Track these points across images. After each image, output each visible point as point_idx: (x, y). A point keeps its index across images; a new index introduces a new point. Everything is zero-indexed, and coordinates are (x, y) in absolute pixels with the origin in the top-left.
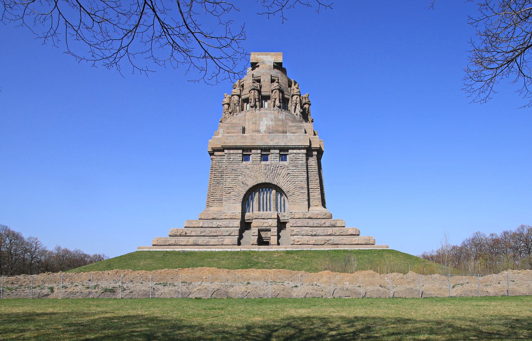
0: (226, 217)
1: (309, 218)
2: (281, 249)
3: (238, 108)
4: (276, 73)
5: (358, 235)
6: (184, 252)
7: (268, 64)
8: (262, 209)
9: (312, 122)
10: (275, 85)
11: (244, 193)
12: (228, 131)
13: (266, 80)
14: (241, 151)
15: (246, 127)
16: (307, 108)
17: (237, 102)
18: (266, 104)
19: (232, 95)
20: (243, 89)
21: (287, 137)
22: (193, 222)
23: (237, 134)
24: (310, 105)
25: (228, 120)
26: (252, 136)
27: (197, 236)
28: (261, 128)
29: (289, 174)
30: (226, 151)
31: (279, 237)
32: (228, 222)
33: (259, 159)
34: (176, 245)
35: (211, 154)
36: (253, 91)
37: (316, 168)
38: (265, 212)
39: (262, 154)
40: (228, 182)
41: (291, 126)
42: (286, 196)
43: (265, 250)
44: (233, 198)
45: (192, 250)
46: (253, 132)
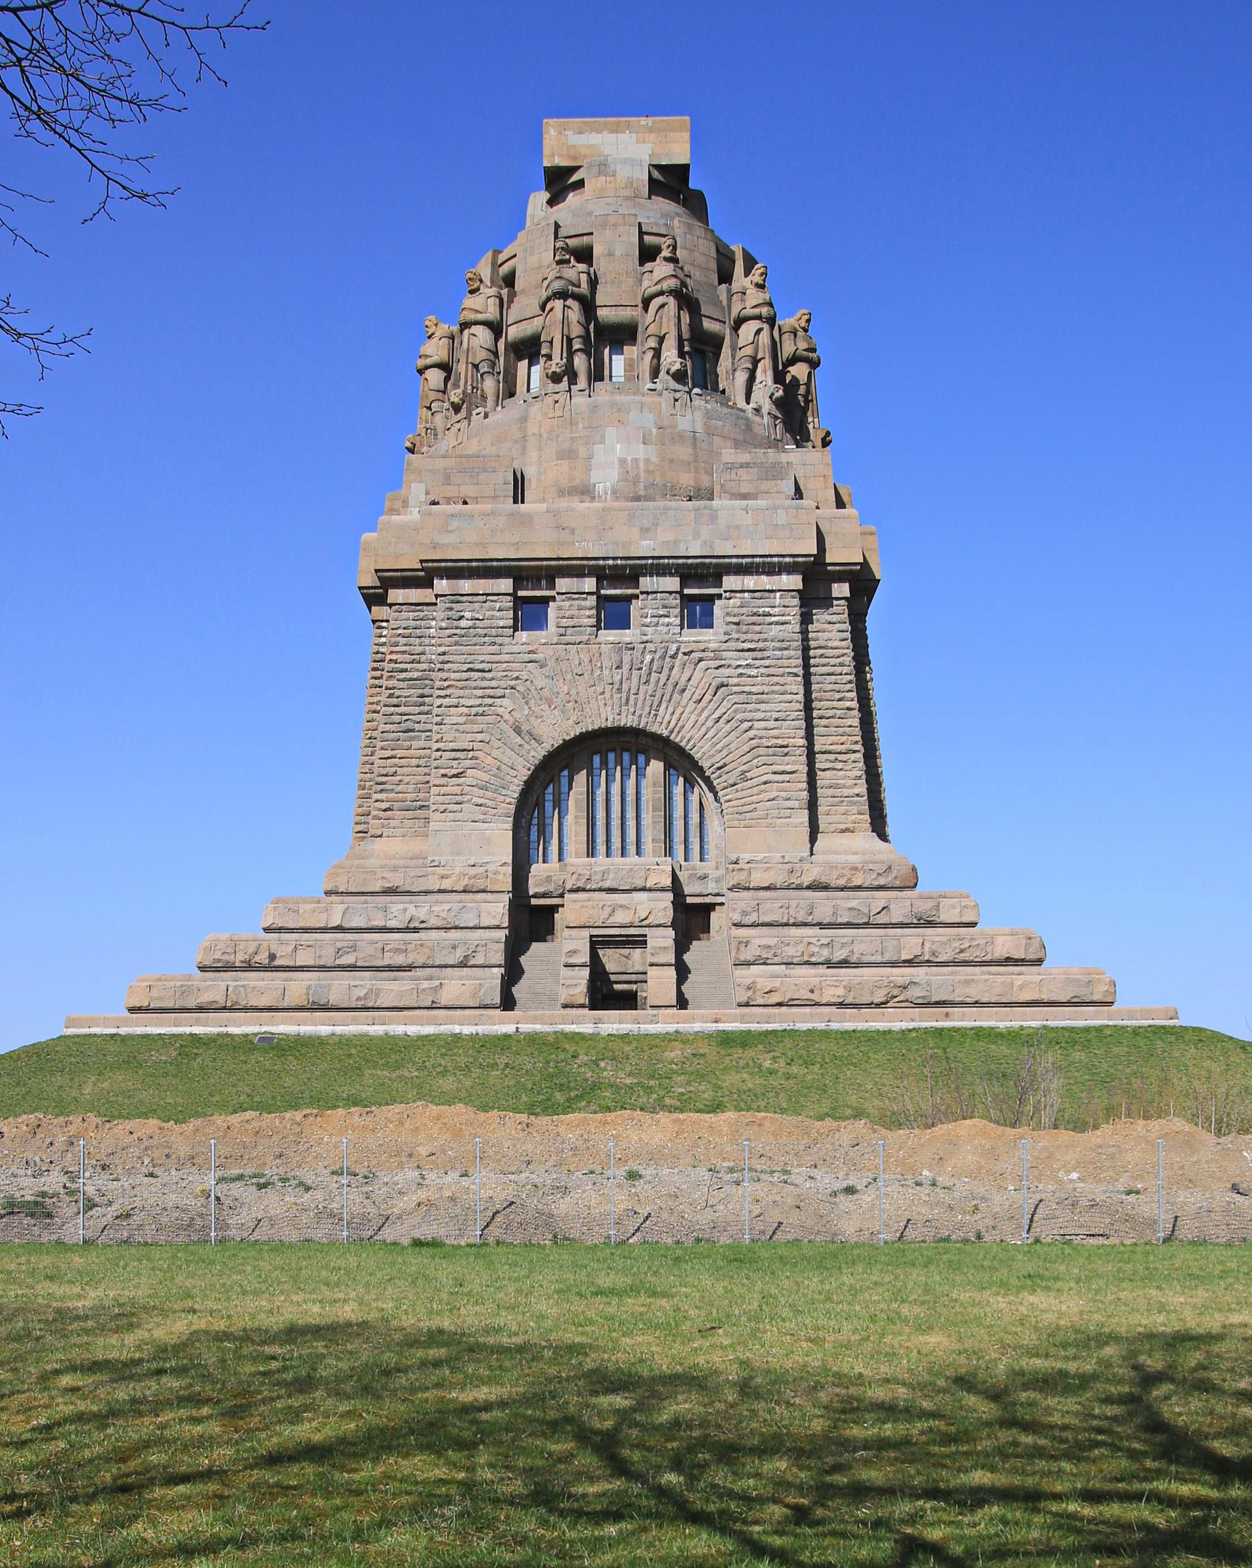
0: (446, 885)
1: (815, 886)
2: (697, 1026)
3: (489, 385)
4: (662, 214)
5: (1039, 962)
6: (267, 1039)
7: (623, 173)
8: (601, 848)
9: (825, 443)
10: (657, 275)
11: (524, 774)
12: (451, 491)
13: (619, 251)
14: (506, 585)
15: (530, 473)
16: (803, 378)
17: (483, 355)
18: (618, 364)
19: (465, 325)
20: (512, 296)
21: (713, 518)
22: (303, 908)
23: (488, 507)
24: (814, 364)
25: (447, 442)
26: (555, 514)
27: (323, 968)
28: (595, 477)
29: (724, 685)
30: (441, 585)
31: (682, 972)
32: (456, 907)
33: (587, 617)
34: (231, 1009)
35: (374, 598)
36: (558, 304)
37: (848, 660)
38: (617, 860)
39: (599, 597)
40: (453, 726)
41: (730, 467)
42: (712, 789)
43: (625, 1028)
44: (477, 796)
45: (306, 1029)
46: (562, 493)
